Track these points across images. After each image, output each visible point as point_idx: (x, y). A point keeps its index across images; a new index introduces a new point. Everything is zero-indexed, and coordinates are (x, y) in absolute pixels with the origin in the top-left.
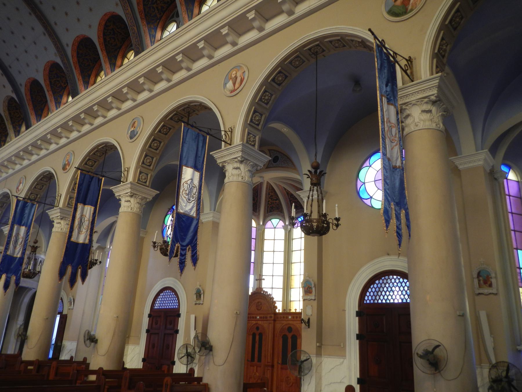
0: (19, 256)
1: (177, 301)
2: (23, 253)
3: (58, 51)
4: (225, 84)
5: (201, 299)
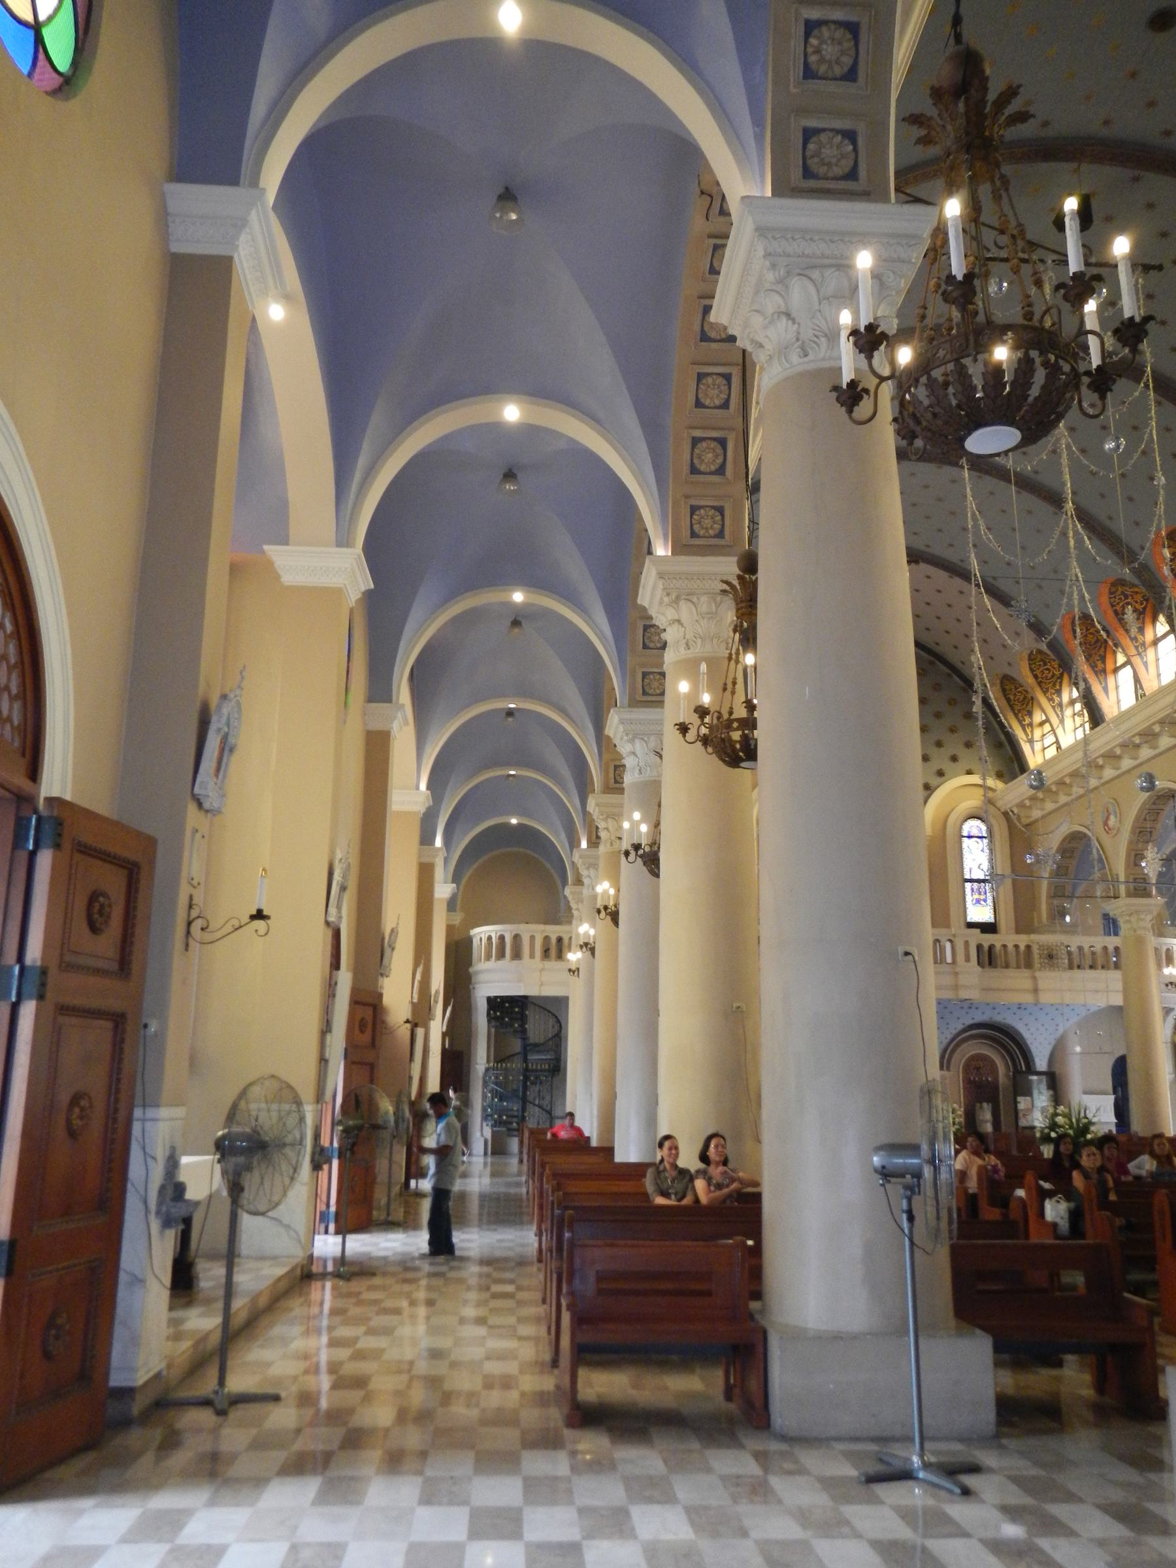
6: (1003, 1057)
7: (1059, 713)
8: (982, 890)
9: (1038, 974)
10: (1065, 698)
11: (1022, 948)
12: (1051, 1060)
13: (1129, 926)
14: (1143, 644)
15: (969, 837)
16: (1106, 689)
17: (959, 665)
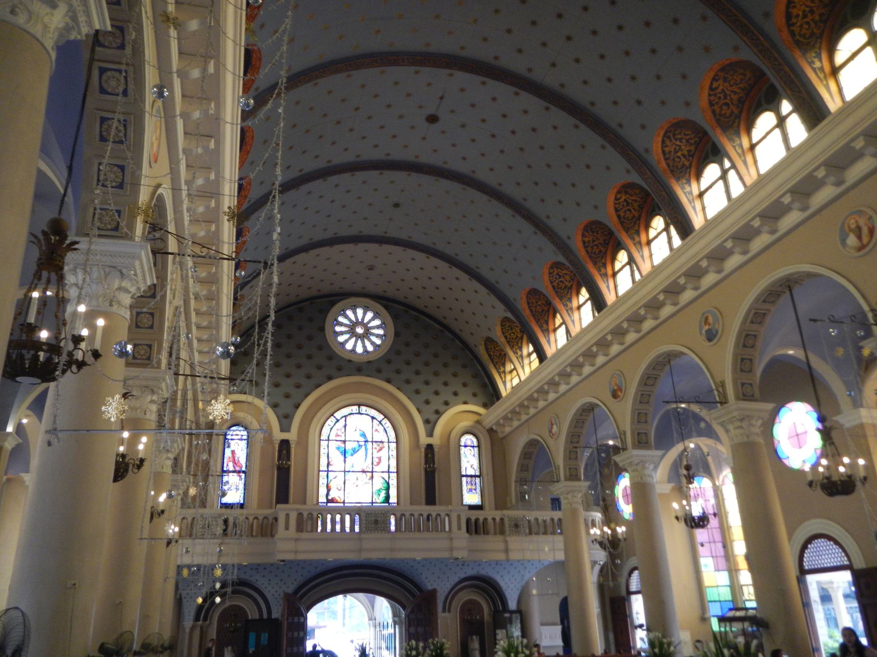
3: (559, 248)
4: (843, 241)
6: (487, 600)
8: (473, 482)
9: (508, 539)
10: (525, 352)
11: (498, 519)
12: (519, 602)
14: (571, 309)
15: (466, 446)
16: (549, 342)
17: (458, 332)
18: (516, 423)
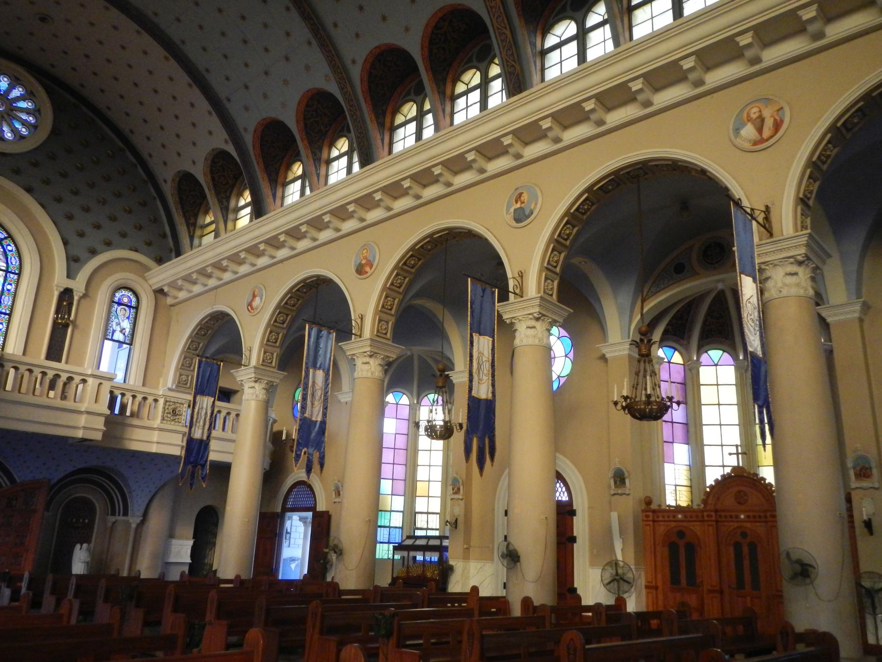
0: (319, 419)
1: (564, 489)
2: (325, 415)
4: (737, 131)
5: (625, 487)
7: (225, 215)
13: (251, 391)
14: (319, 160)
15: (120, 304)
17: (146, 156)
18: (197, 289)
